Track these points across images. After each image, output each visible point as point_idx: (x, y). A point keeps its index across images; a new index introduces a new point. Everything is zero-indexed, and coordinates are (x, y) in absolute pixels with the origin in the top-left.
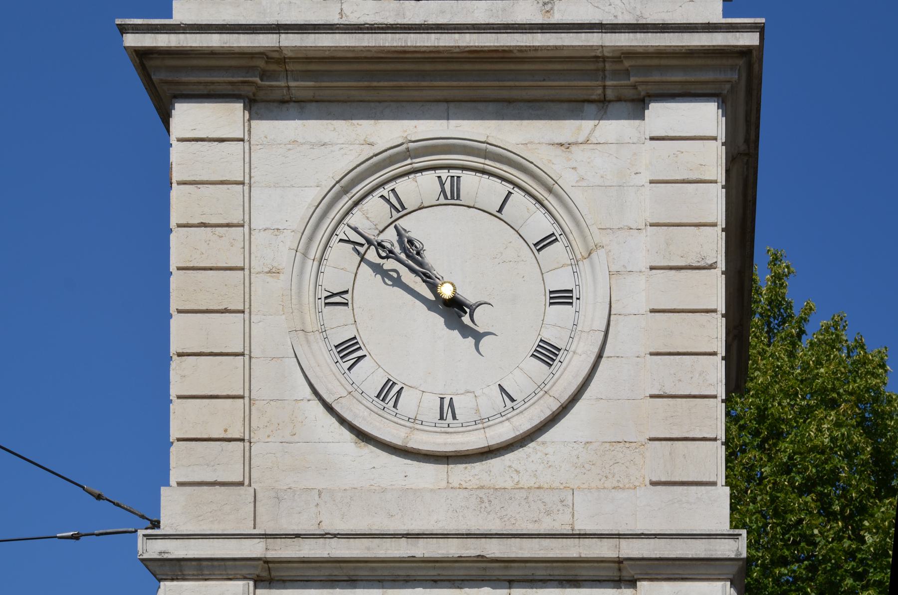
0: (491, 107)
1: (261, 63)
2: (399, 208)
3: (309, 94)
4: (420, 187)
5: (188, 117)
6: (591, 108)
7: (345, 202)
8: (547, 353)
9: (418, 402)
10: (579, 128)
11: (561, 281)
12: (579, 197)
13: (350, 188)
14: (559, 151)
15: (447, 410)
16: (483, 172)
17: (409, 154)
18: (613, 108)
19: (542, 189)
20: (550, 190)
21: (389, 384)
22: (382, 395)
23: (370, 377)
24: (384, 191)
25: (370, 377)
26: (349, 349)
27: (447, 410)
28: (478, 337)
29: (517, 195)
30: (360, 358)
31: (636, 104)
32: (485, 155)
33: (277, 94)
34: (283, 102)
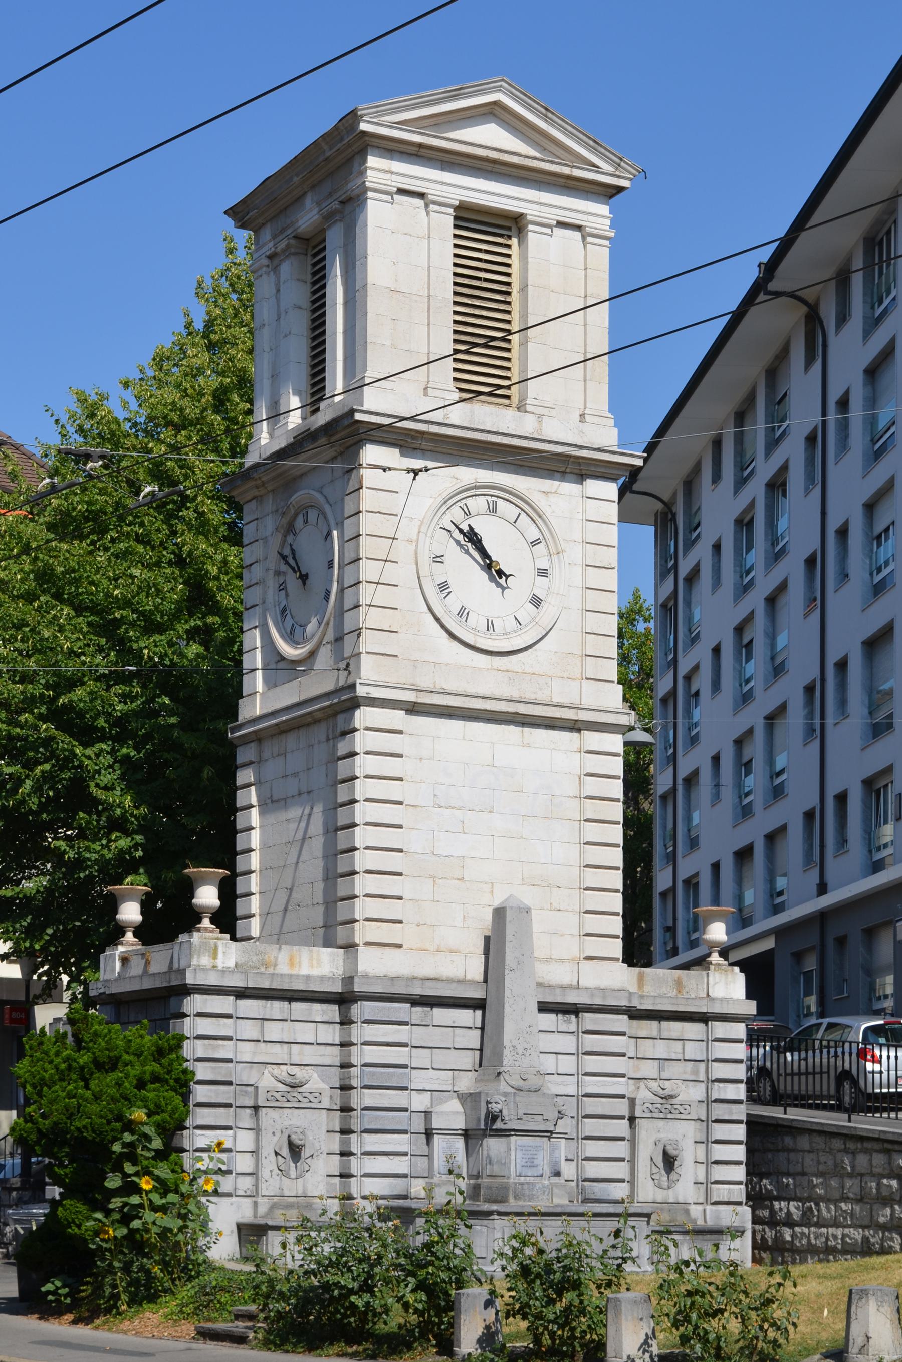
0: (512, 467)
1: (413, 433)
2: (468, 513)
3: (430, 448)
4: (478, 504)
5: (371, 454)
6: (558, 475)
7: (444, 508)
8: (536, 602)
9: (477, 620)
10: (552, 484)
11: (543, 564)
12: (553, 521)
13: (447, 502)
14: (543, 495)
15: (490, 626)
16: (507, 500)
17: (476, 487)
18: (568, 476)
19: (536, 515)
20: (540, 517)
21: (463, 609)
22: (460, 614)
23: (454, 602)
24: (461, 504)
25: (454, 602)
26: (443, 586)
27: (490, 626)
28: (503, 589)
29: (523, 515)
30: (450, 593)
31: (581, 477)
32: (510, 493)
33: (414, 446)
34: (415, 449)
